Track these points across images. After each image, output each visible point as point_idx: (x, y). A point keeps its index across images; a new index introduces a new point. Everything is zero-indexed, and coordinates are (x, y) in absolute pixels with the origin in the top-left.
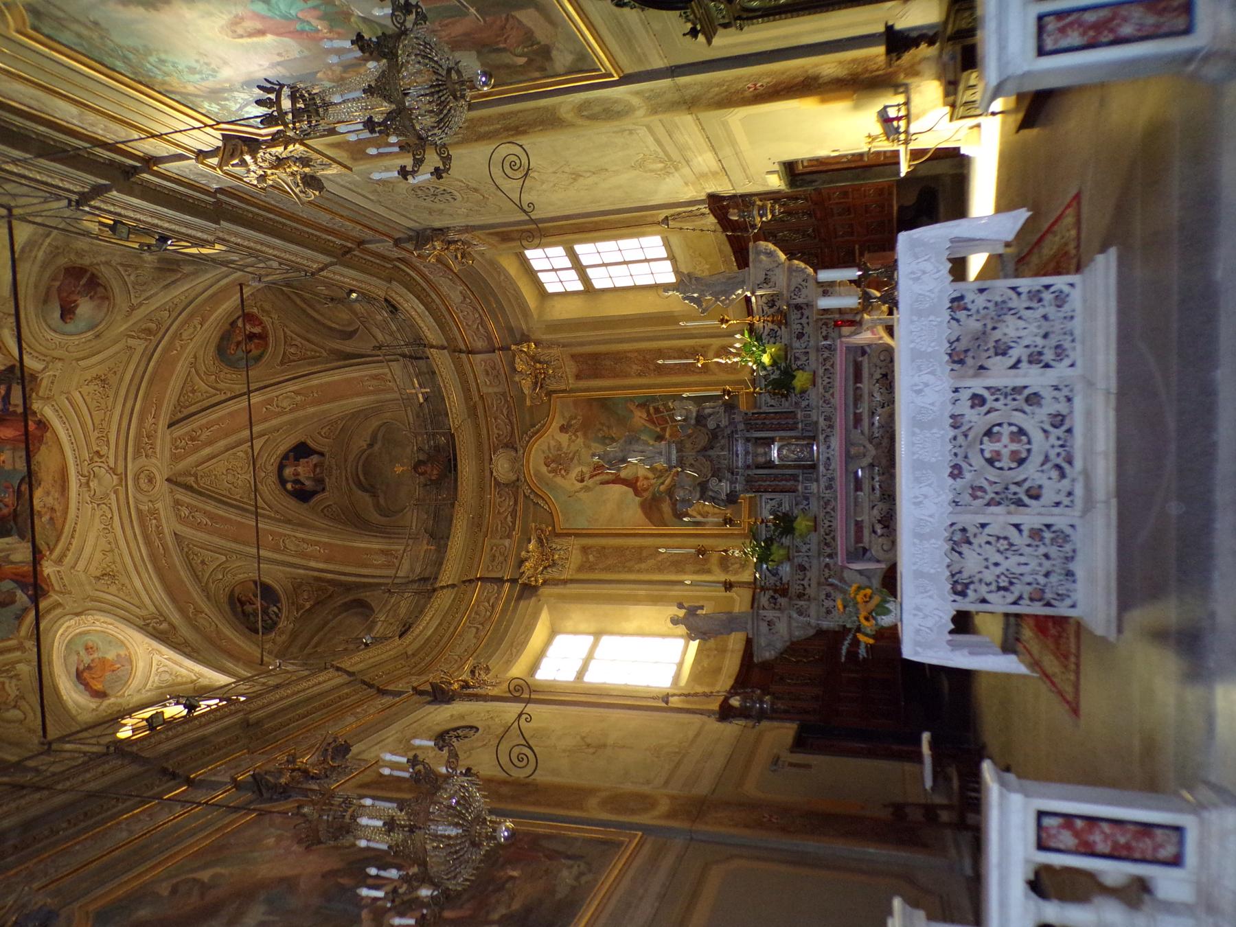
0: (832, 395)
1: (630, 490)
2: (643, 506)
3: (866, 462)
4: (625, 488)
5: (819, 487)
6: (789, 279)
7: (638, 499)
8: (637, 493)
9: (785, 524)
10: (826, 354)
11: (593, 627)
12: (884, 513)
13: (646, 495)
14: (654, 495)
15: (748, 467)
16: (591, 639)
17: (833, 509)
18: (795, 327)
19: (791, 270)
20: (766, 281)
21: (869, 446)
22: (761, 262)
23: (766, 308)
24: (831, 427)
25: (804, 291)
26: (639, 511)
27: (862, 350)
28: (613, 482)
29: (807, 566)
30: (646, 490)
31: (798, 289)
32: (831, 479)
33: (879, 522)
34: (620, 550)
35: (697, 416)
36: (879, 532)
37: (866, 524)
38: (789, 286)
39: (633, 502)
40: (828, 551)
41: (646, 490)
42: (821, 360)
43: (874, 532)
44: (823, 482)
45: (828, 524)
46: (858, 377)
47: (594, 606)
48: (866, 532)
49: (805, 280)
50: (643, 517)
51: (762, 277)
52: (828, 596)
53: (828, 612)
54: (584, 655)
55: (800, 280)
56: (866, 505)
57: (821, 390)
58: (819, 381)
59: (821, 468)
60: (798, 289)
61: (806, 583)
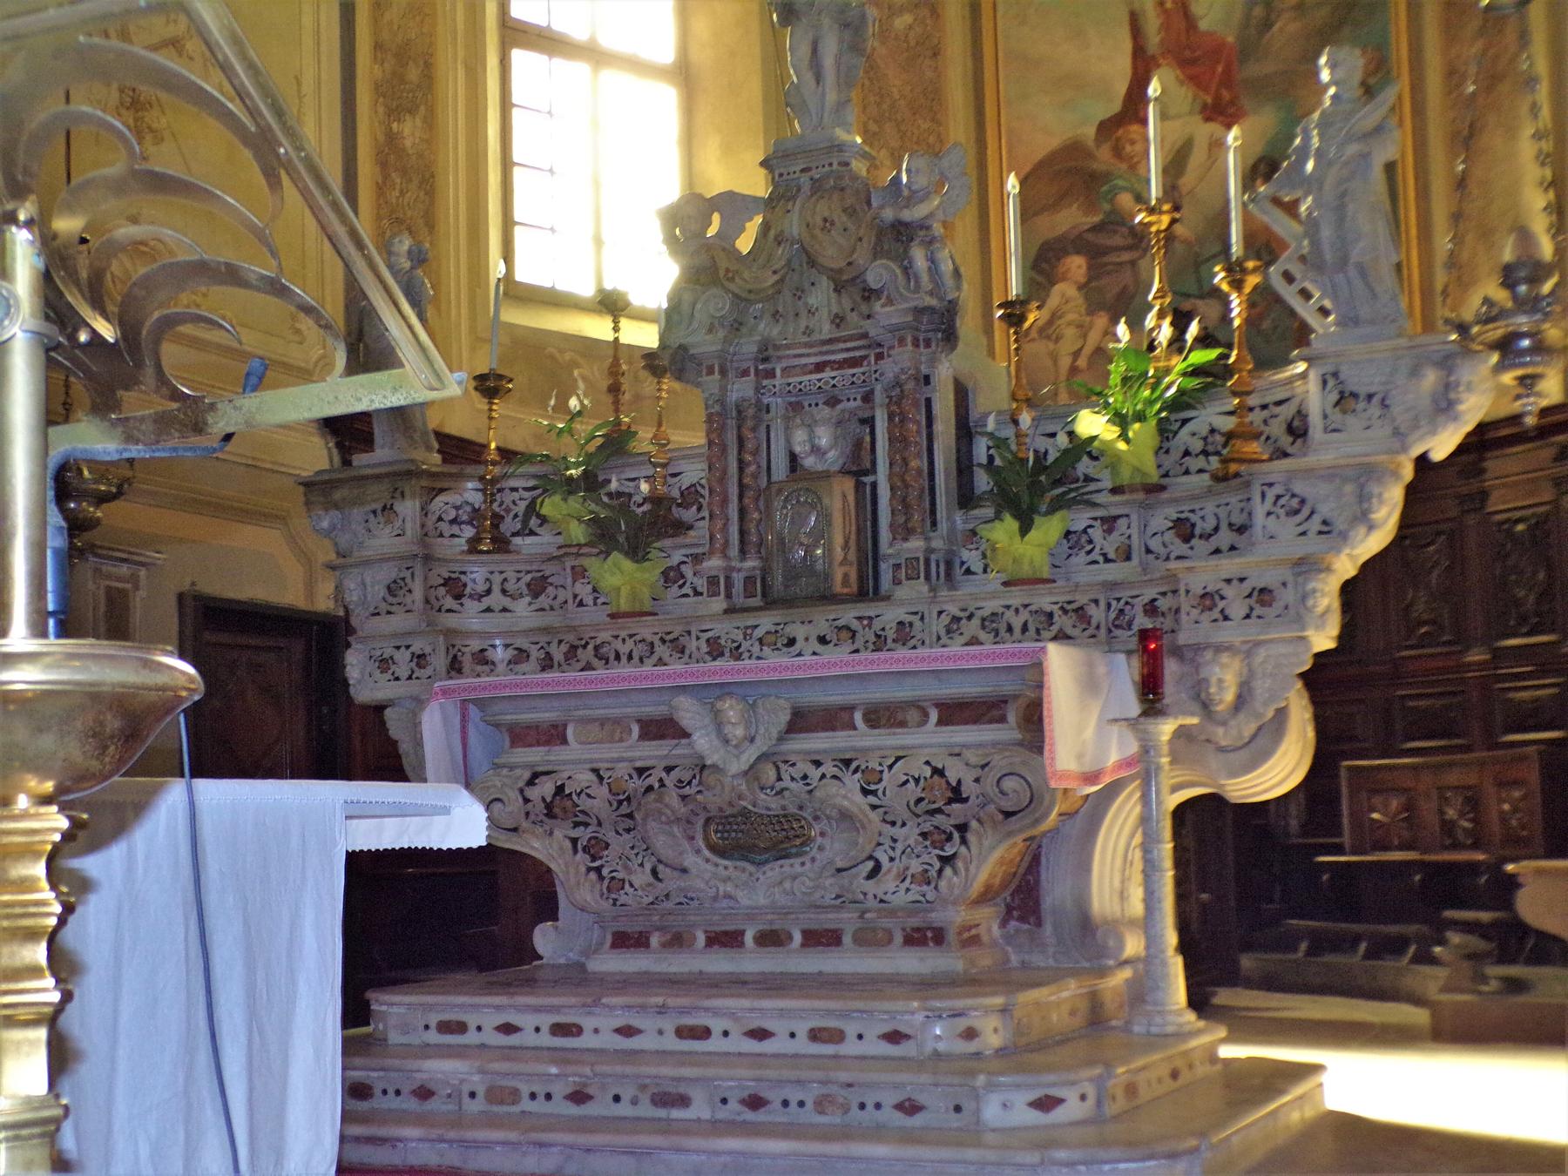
0: (974, 641)
1: (1116, 106)
2: (1073, 149)
3: (703, 742)
4: (1121, 88)
5: (712, 617)
6: (1332, 474)
7: (1090, 131)
8: (1108, 128)
9: (639, 528)
10: (1097, 614)
11: (702, 56)
12: (584, 803)
13: (1104, 153)
14: (1106, 177)
16: (665, 52)
17: (661, 662)
18: (1210, 507)
19: (1366, 476)
20: (1345, 399)
21: (750, 755)
22: (1415, 372)
23: (1287, 411)
24: (880, 643)
25: (1286, 528)
26: (1055, 143)
27: (1034, 718)
28: (1139, 52)
29: (543, 601)
30: (1118, 152)
31: (1298, 508)
32: (737, 654)
33: (560, 789)
34: (930, 101)
35: (906, 225)
36: (534, 793)
37: (558, 754)
38: (1309, 472)
39: (1078, 121)
40: (558, 654)
41: (1118, 152)
42: (1082, 599)
44: (728, 630)
45: (624, 649)
46: (954, 712)
47: (757, 50)
48: (534, 756)
49: (1327, 528)
50: (1040, 155)
51: (1358, 380)
52: (420, 659)
53: (385, 664)
54: (607, 42)
55: (1325, 510)
56: (604, 753)
57: (991, 606)
58: (1016, 597)
59: (766, 622)
60: (1298, 508)
61: (497, 599)
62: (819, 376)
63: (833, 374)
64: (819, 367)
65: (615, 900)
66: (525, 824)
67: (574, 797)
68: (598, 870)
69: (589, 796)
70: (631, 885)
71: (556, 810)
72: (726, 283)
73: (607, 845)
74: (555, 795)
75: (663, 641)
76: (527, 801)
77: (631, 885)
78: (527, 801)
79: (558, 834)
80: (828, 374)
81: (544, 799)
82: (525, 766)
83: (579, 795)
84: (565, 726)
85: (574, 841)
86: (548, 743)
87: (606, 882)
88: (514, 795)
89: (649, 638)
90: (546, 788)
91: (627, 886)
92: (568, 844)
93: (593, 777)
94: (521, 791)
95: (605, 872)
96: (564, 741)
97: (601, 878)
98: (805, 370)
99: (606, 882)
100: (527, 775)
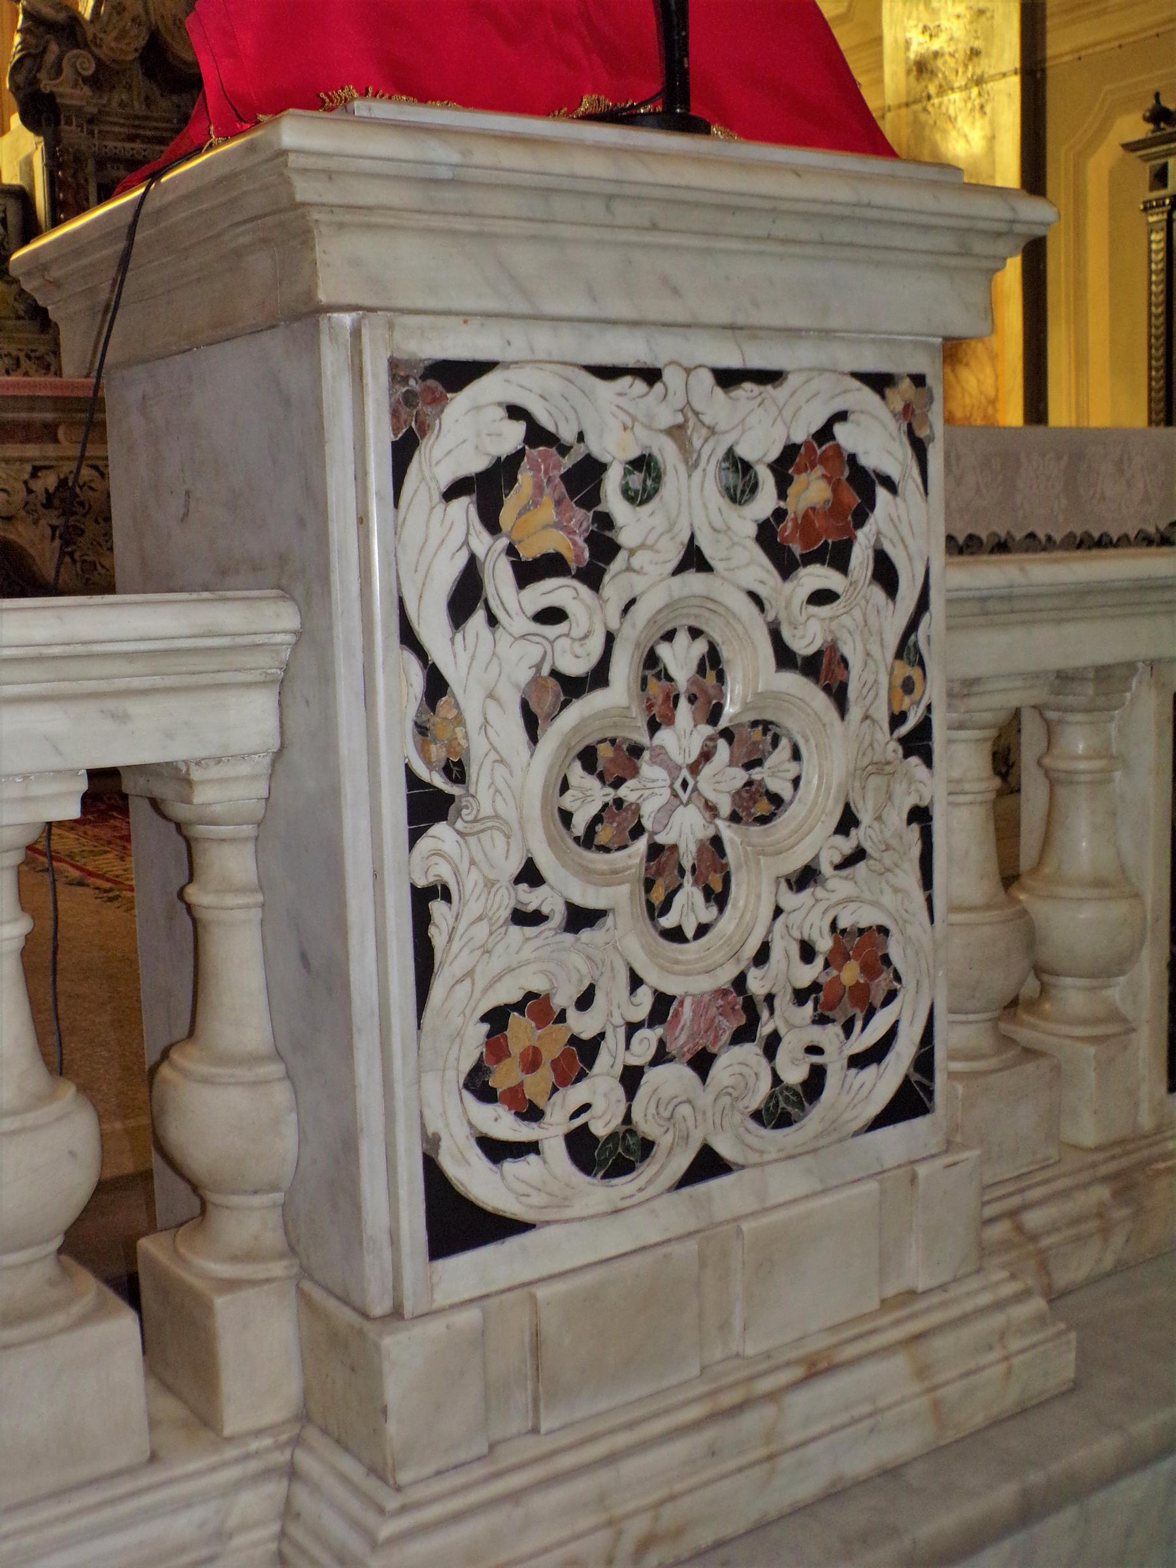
15: (101, 163)
33: (63, 483)
36: (38, 486)
43: (35, 472)
48: (32, 451)
62: (132, 145)
63: (144, 146)
64: (131, 138)
65: (88, 579)
66: (23, 513)
67: (77, 490)
68: (71, 554)
69: (91, 488)
70: (103, 566)
71: (56, 502)
72: (93, 48)
73: (83, 532)
74: (57, 489)
75: (28, 357)
76: (30, 491)
77: (103, 566)
78: (30, 491)
79: (43, 522)
80: (138, 145)
81: (47, 490)
82: (22, 460)
83: (81, 488)
84: (57, 426)
85: (54, 528)
86: (39, 439)
87: (79, 565)
88: (20, 486)
89: (14, 353)
90: (49, 481)
91: (99, 568)
92: (48, 531)
93: (96, 474)
94: (26, 482)
95: (77, 556)
96: (56, 440)
97: (74, 561)
98: (117, 137)
99: (79, 565)
100: (28, 468)
